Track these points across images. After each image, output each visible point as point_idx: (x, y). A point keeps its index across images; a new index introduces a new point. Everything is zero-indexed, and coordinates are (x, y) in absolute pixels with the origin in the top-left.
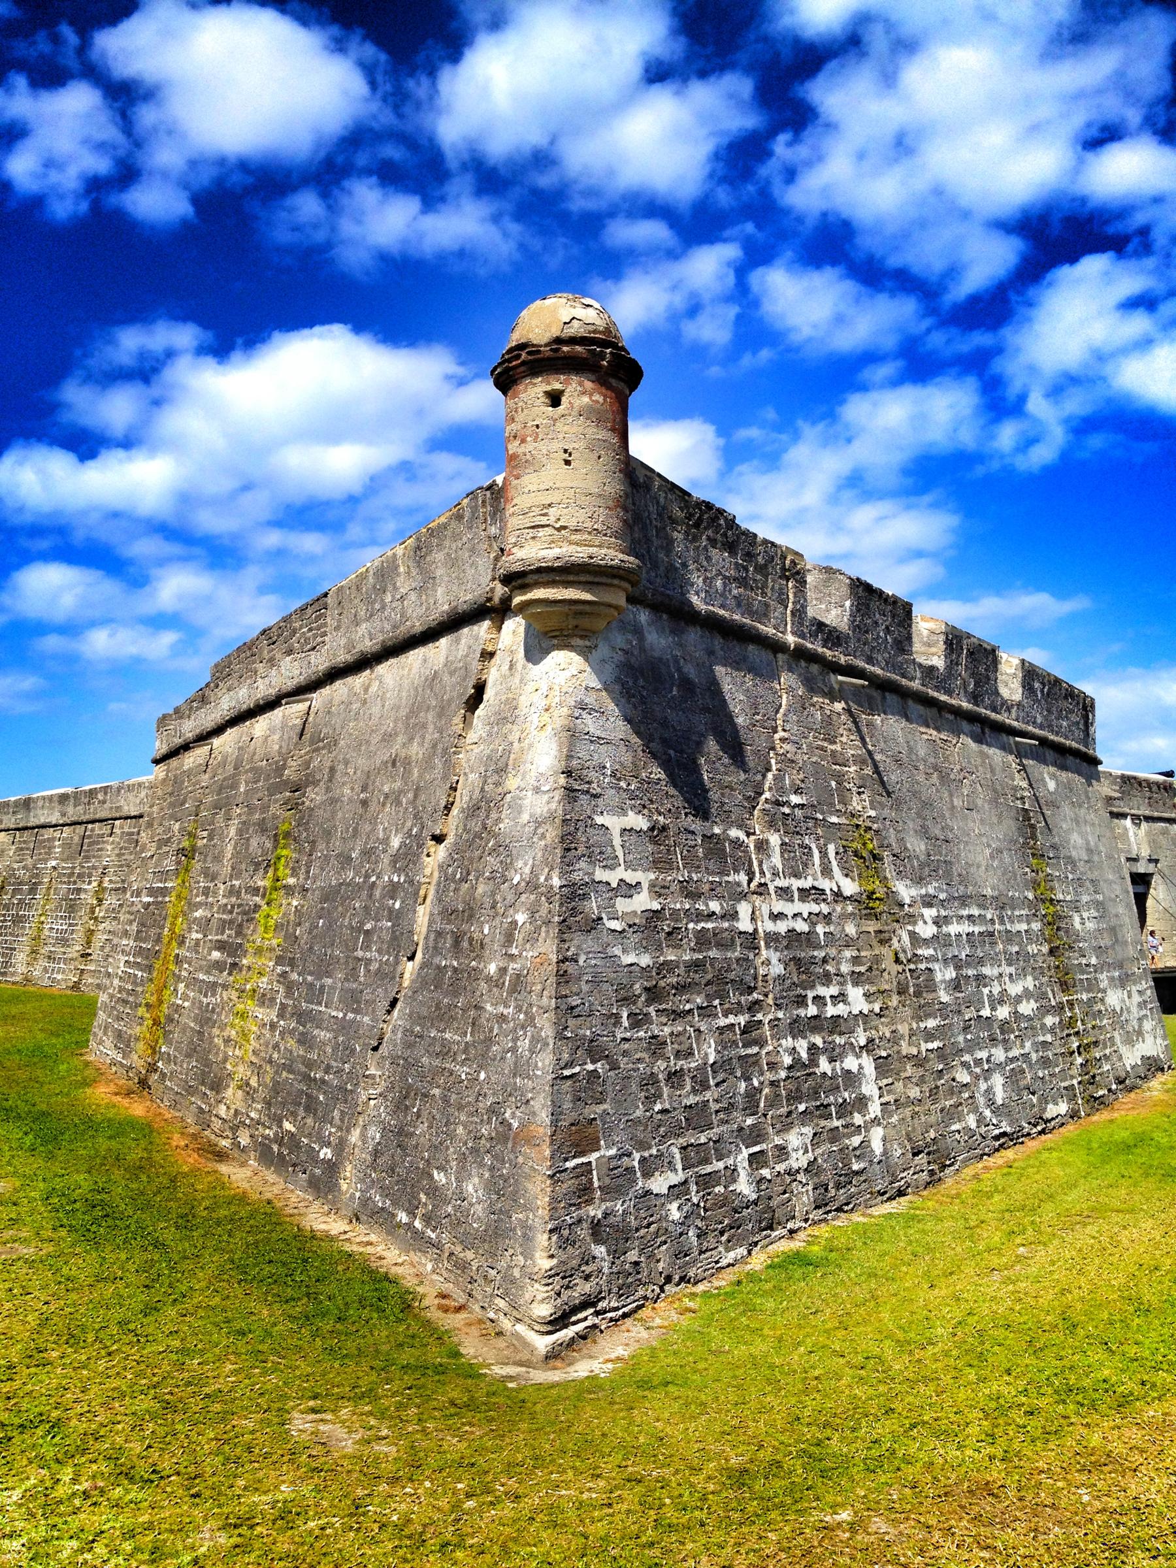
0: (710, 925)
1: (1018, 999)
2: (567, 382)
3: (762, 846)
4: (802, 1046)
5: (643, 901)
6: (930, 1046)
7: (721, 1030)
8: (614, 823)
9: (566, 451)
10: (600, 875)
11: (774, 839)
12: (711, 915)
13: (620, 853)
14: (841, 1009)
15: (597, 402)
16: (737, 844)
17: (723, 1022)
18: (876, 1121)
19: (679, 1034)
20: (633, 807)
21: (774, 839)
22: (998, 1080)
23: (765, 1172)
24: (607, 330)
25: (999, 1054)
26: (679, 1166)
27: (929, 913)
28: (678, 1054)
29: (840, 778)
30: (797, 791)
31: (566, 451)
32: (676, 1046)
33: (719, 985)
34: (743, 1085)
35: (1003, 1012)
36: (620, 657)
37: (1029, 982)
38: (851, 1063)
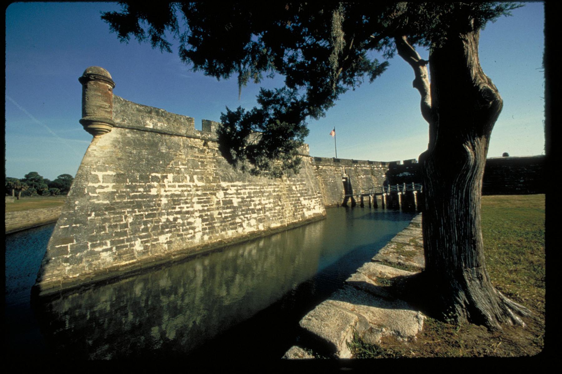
1: (266, 204)
4: (171, 218)
6: (226, 215)
12: (140, 192)
13: (101, 179)
17: (138, 213)
23: (149, 244)
25: (255, 215)
27: (232, 188)
30: (183, 165)
33: (139, 206)
34: (143, 227)
35: (258, 207)
37: (272, 200)
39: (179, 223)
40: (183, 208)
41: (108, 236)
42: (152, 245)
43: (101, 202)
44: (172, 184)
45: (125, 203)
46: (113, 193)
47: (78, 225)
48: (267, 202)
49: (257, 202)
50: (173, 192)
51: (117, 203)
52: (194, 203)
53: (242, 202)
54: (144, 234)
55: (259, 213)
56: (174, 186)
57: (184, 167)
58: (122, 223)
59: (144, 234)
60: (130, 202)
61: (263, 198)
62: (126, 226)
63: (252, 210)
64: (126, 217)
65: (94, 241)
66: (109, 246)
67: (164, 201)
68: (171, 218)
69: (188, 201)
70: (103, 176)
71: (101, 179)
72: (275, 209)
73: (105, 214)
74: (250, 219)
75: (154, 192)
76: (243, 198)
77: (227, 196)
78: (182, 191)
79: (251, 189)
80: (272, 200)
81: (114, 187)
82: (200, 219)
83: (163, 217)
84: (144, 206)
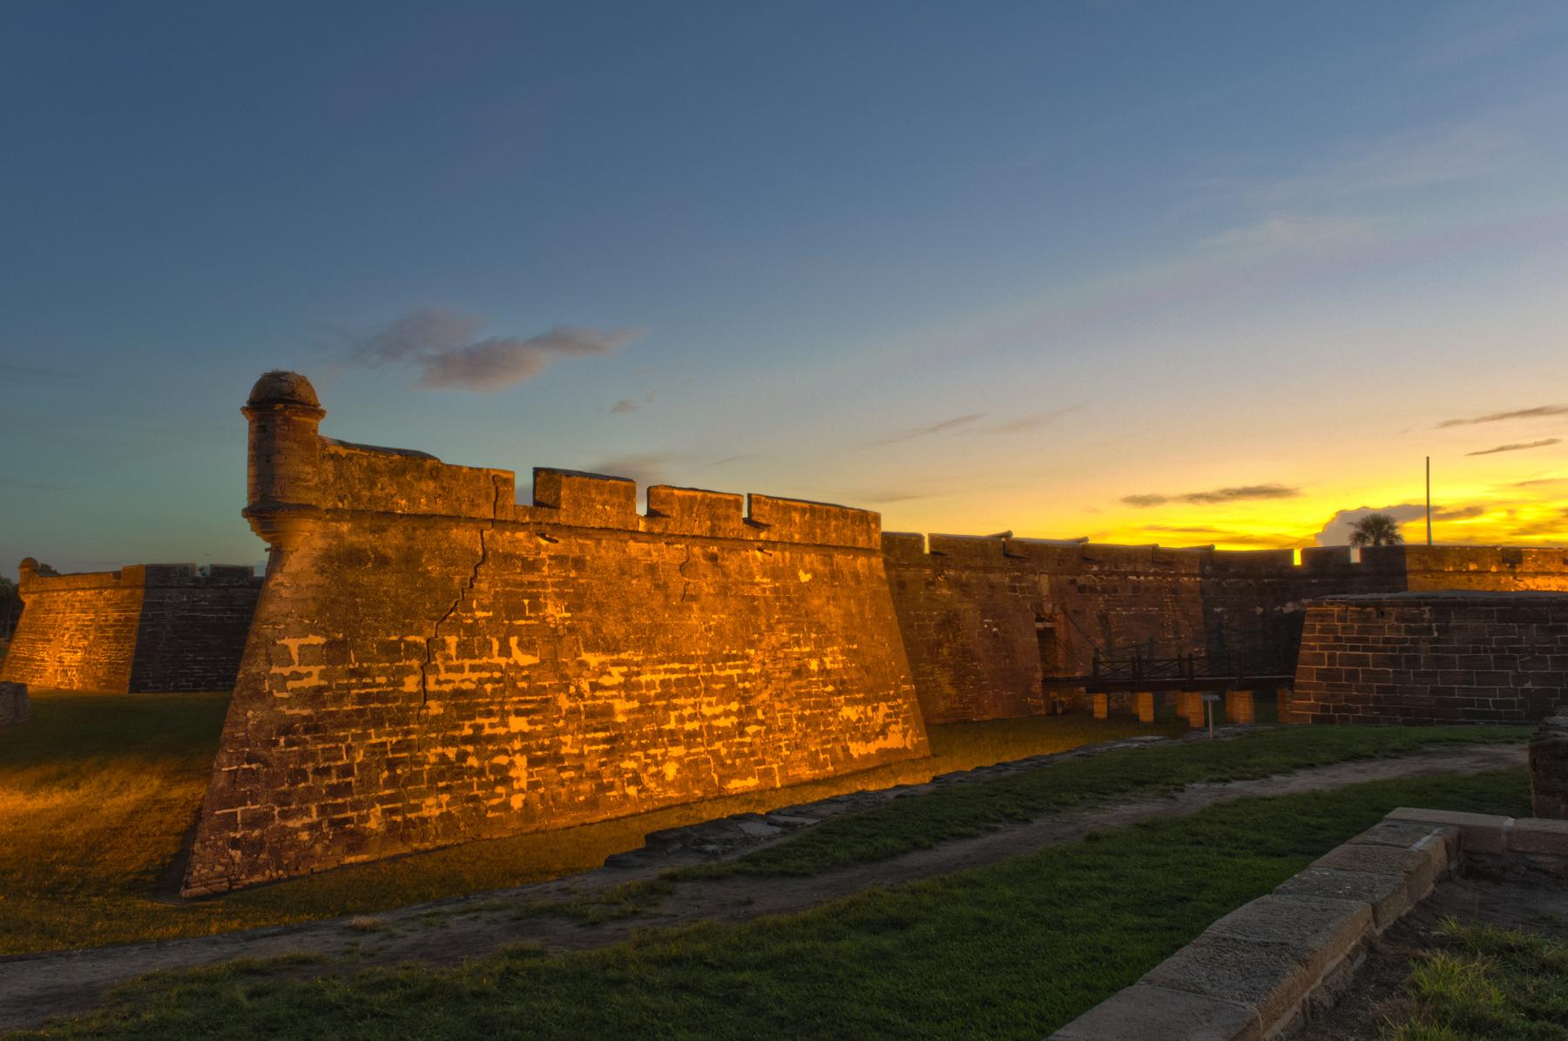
0: (375, 690)
1: (716, 717)
3: (436, 644)
5: (314, 681)
7: (374, 745)
8: (293, 644)
10: (275, 670)
11: (452, 640)
12: (379, 685)
13: (295, 657)
14: (501, 731)
16: (415, 645)
17: (374, 740)
18: (521, 791)
21: (452, 640)
22: (671, 770)
23: (399, 819)
26: (314, 815)
27: (615, 671)
29: (534, 598)
30: (483, 608)
33: (377, 721)
34: (386, 774)
35: (689, 726)
36: (315, 554)
37: (734, 706)
38: (502, 760)
39: (471, 767)
40: (481, 727)
42: (406, 821)
43: (296, 711)
44: (455, 662)
45: (348, 715)
46: (319, 690)
47: (254, 766)
48: (720, 709)
49: (687, 712)
50: (457, 685)
51: (331, 714)
52: (508, 713)
53: (640, 710)
54: (387, 792)
55: (689, 746)
56: (460, 669)
57: (485, 614)
59: (387, 792)
61: (706, 699)
62: (347, 771)
63: (672, 732)
64: (349, 748)
67: (435, 708)
68: (451, 753)
69: (494, 708)
70: (301, 647)
71: (295, 657)
72: (742, 734)
73: (306, 742)
74: (664, 762)
75: (411, 684)
76: (644, 700)
77: (598, 693)
78: (481, 681)
79: (673, 671)
80: (734, 706)
81: (322, 675)
82: (525, 759)
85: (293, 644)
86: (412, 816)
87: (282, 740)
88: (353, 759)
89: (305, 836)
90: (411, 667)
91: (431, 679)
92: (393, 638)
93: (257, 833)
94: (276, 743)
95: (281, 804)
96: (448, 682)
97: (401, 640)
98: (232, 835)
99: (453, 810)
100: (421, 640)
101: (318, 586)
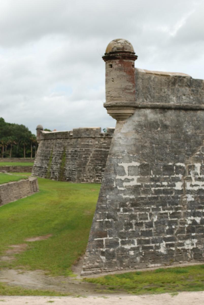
0: (162, 188)
2: (113, 62)
5: (135, 183)
8: (126, 165)
9: (112, 79)
10: (118, 177)
11: (198, 165)
12: (163, 186)
13: (127, 172)
15: (119, 66)
16: (180, 167)
17: (162, 212)
19: (143, 214)
20: (134, 160)
23: (173, 249)
24: (123, 48)
26: (136, 243)
28: (141, 219)
31: (112, 79)
32: (141, 217)
36: (135, 124)
41: (134, 234)
43: (127, 196)
45: (150, 199)
47: (110, 220)
50: (201, 187)
51: (142, 198)
54: (168, 236)
58: (147, 221)
59: (168, 236)
60: (154, 198)
62: (150, 225)
64: (151, 215)
65: (123, 238)
66: (136, 245)
67: (190, 198)
70: (129, 167)
71: (127, 172)
73: (131, 210)
75: (178, 186)
81: (139, 180)
83: (189, 218)
84: (169, 203)
85: (126, 165)
86: (180, 248)
87: (122, 209)
88: (153, 220)
89: (132, 253)
90: (178, 178)
91: (188, 184)
92: (170, 164)
93: (112, 250)
94: (119, 210)
95: (122, 238)
96: (196, 185)
97: (174, 165)
98: (101, 249)
99: (200, 247)
100: (183, 165)
101: (136, 139)
